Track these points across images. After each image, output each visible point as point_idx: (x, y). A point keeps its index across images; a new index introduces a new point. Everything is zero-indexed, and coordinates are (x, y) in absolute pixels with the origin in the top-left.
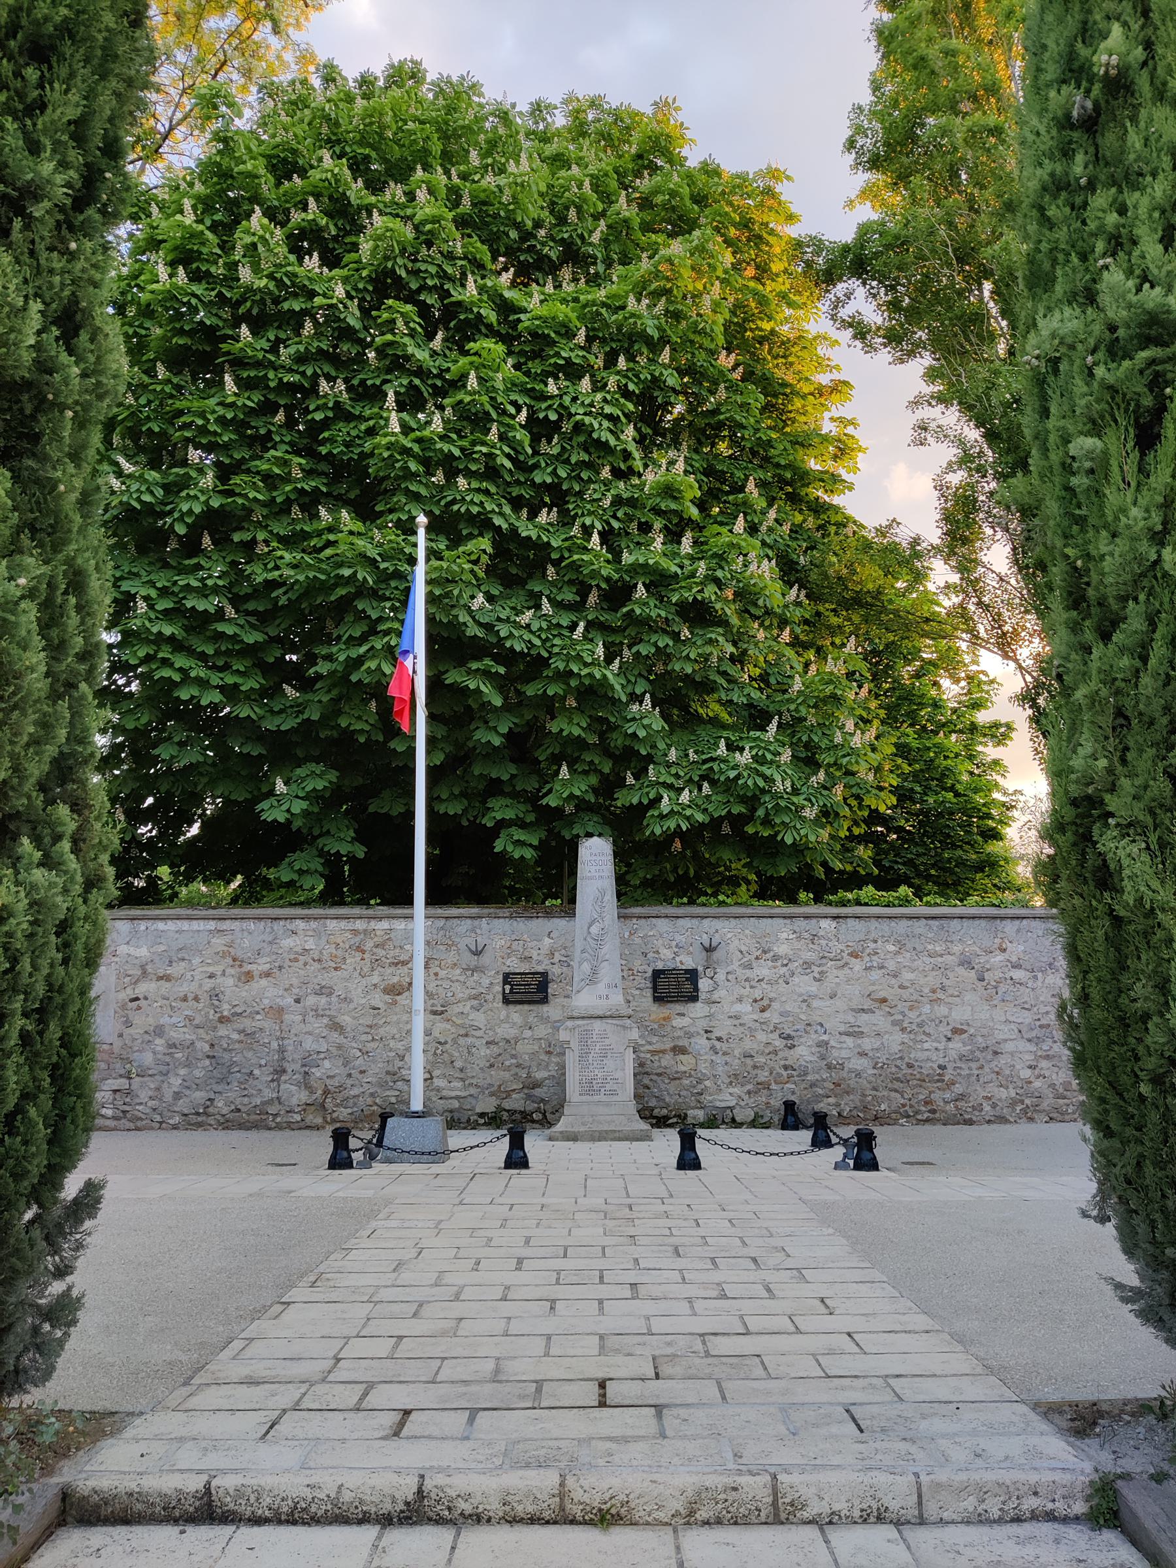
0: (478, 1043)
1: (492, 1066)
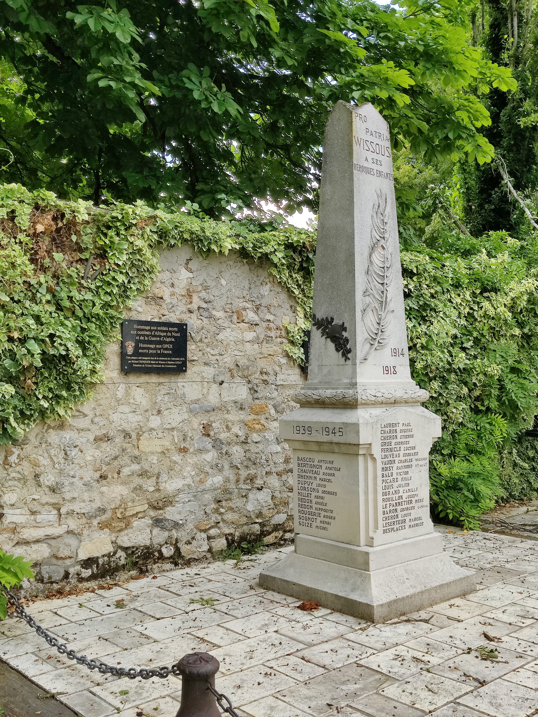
0: (81, 439)
1: (103, 477)
